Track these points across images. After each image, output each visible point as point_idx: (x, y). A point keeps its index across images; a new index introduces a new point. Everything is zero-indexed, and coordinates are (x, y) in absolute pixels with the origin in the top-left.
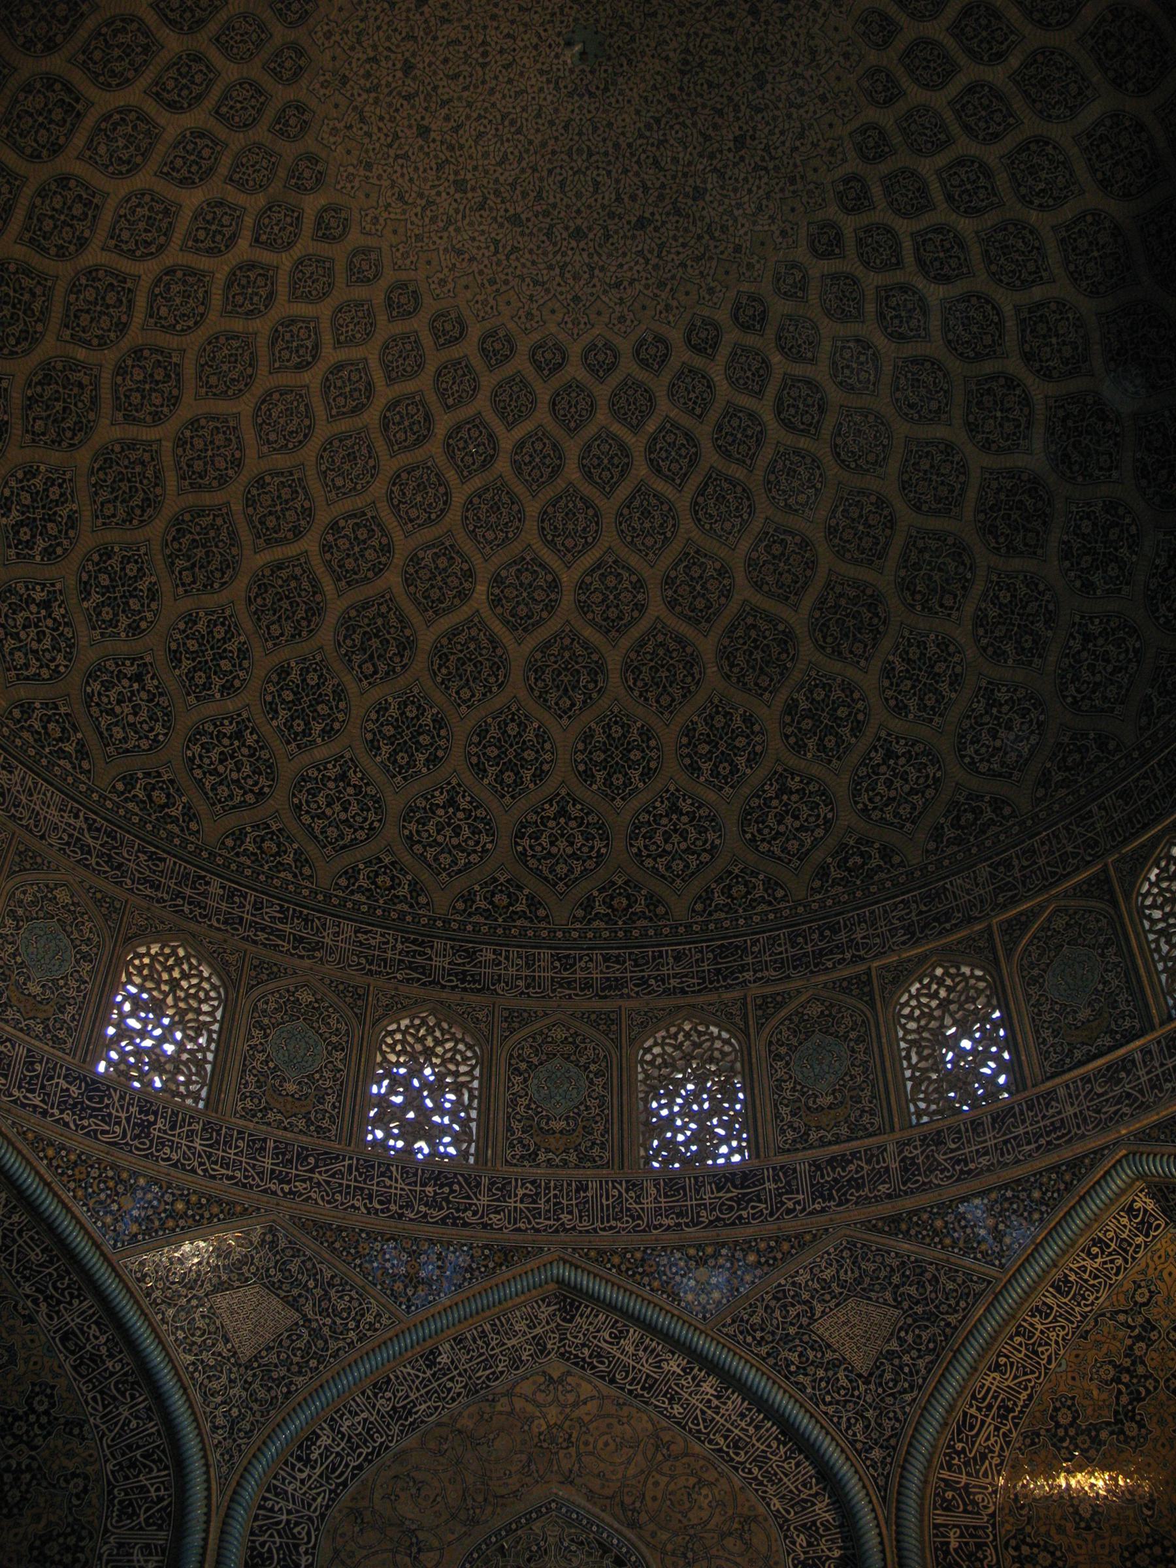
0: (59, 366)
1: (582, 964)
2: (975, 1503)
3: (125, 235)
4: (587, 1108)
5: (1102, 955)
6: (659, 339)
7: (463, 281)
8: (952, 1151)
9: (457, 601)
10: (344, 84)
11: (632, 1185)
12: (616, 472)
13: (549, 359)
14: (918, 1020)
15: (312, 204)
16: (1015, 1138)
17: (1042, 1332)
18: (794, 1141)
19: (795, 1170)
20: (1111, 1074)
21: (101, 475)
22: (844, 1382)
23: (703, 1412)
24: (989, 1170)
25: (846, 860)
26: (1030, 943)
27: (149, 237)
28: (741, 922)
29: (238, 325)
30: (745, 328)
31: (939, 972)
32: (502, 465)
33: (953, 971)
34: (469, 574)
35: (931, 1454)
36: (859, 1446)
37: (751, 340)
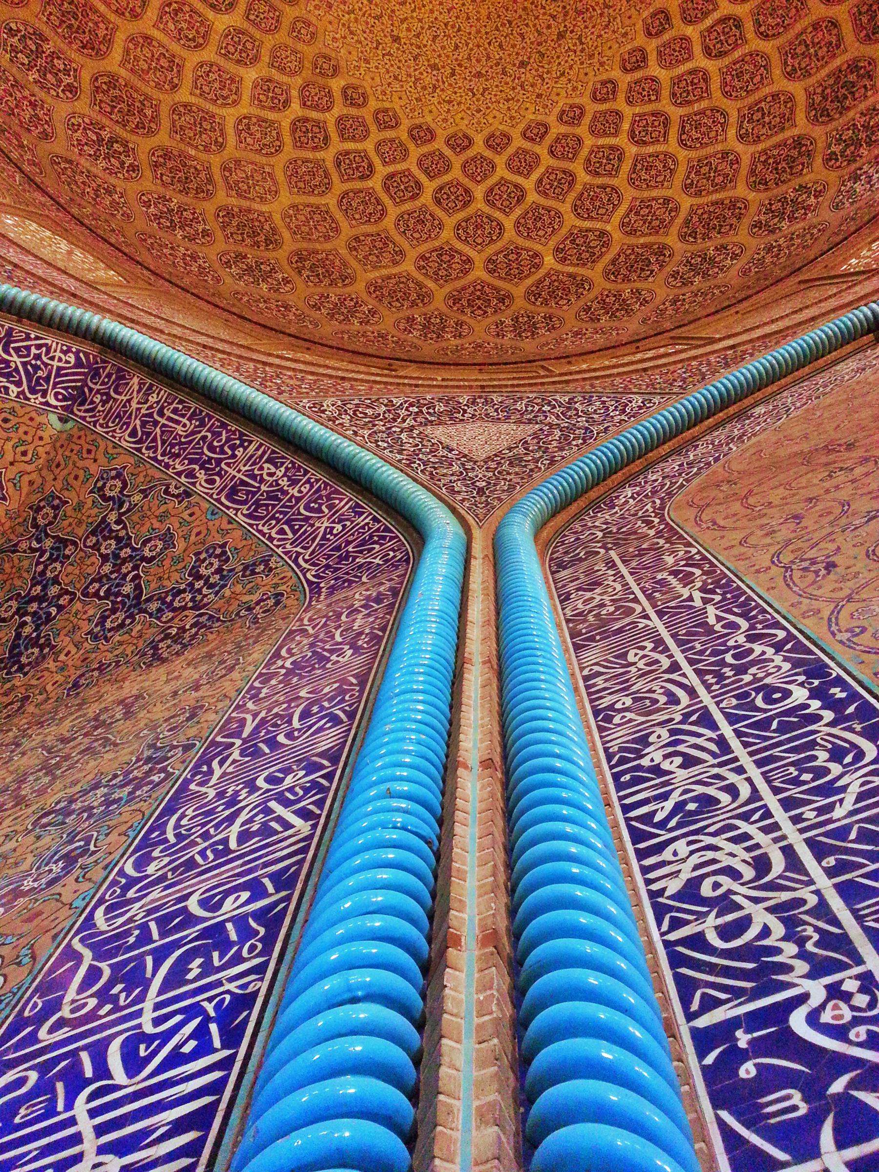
0: (177, 153)
3: (206, 89)
6: (604, 83)
7: (460, 115)
9: (533, 270)
10: (330, 7)
12: (615, 162)
13: (536, 132)
15: (336, 85)
21: (227, 219)
27: (225, 93)
29: (310, 155)
30: (659, 34)
32: (532, 197)
34: (536, 255)
37: (666, 37)
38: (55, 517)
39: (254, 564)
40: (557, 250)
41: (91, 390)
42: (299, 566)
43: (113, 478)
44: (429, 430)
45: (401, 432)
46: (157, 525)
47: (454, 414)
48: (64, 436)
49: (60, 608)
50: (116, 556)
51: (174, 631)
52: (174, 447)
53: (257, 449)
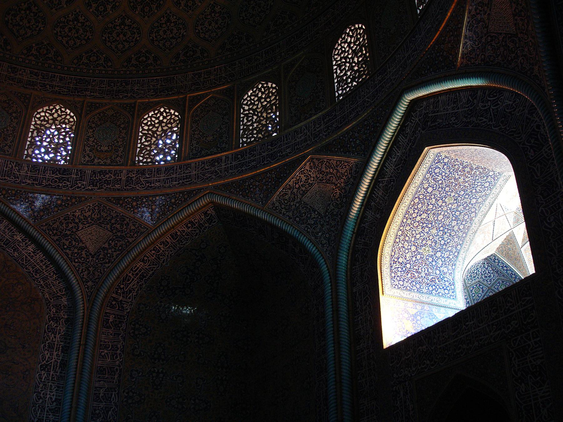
1: (21, 72)
2: (123, 307)
4: (7, 130)
5: (223, 118)
8: (147, 178)
11: (18, 165)
14: (149, 126)
16: (171, 178)
17: (163, 251)
18: (88, 161)
19: (85, 172)
20: (212, 163)
22: (84, 255)
23: (26, 257)
24: (158, 188)
25: (140, 57)
26: (199, 107)
28: (91, 71)
31: (162, 110)
33: (167, 111)
35: (110, 288)
36: (84, 280)
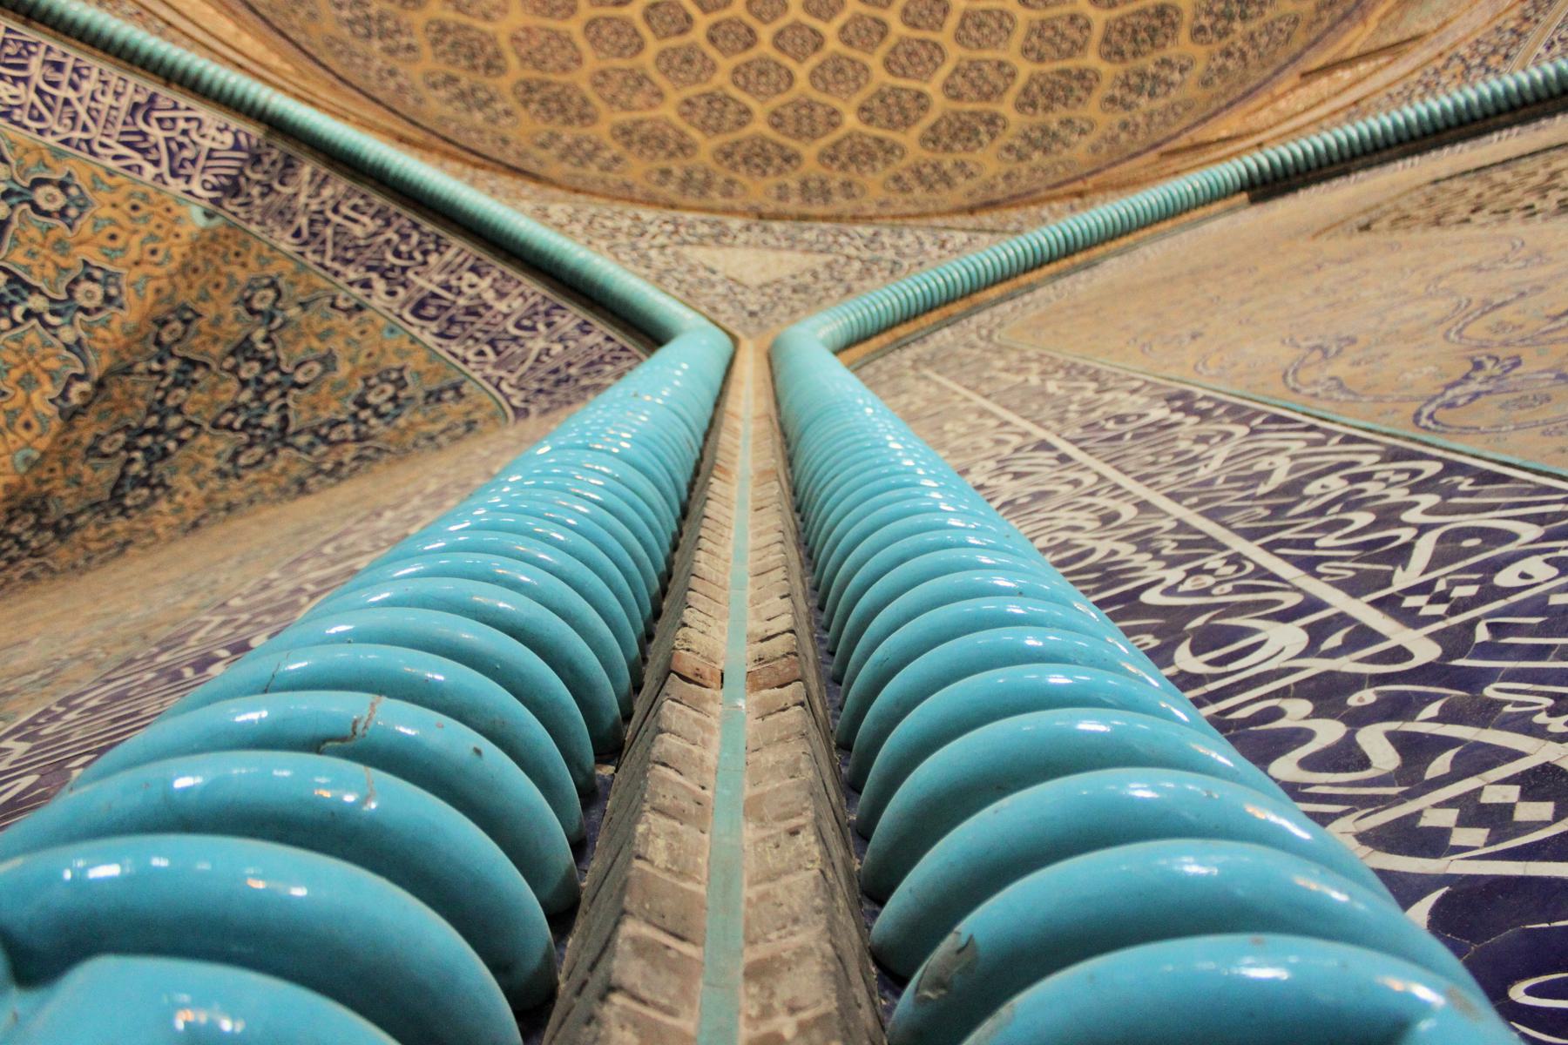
32: (833, 45)
34: (834, 112)
38: (185, 332)
39: (441, 391)
40: (863, 109)
41: (248, 179)
42: (500, 391)
43: (267, 287)
44: (686, 250)
45: (651, 247)
46: (316, 344)
47: (720, 237)
48: (208, 234)
49: (181, 442)
50: (259, 381)
51: (327, 466)
52: (348, 251)
53: (458, 255)
